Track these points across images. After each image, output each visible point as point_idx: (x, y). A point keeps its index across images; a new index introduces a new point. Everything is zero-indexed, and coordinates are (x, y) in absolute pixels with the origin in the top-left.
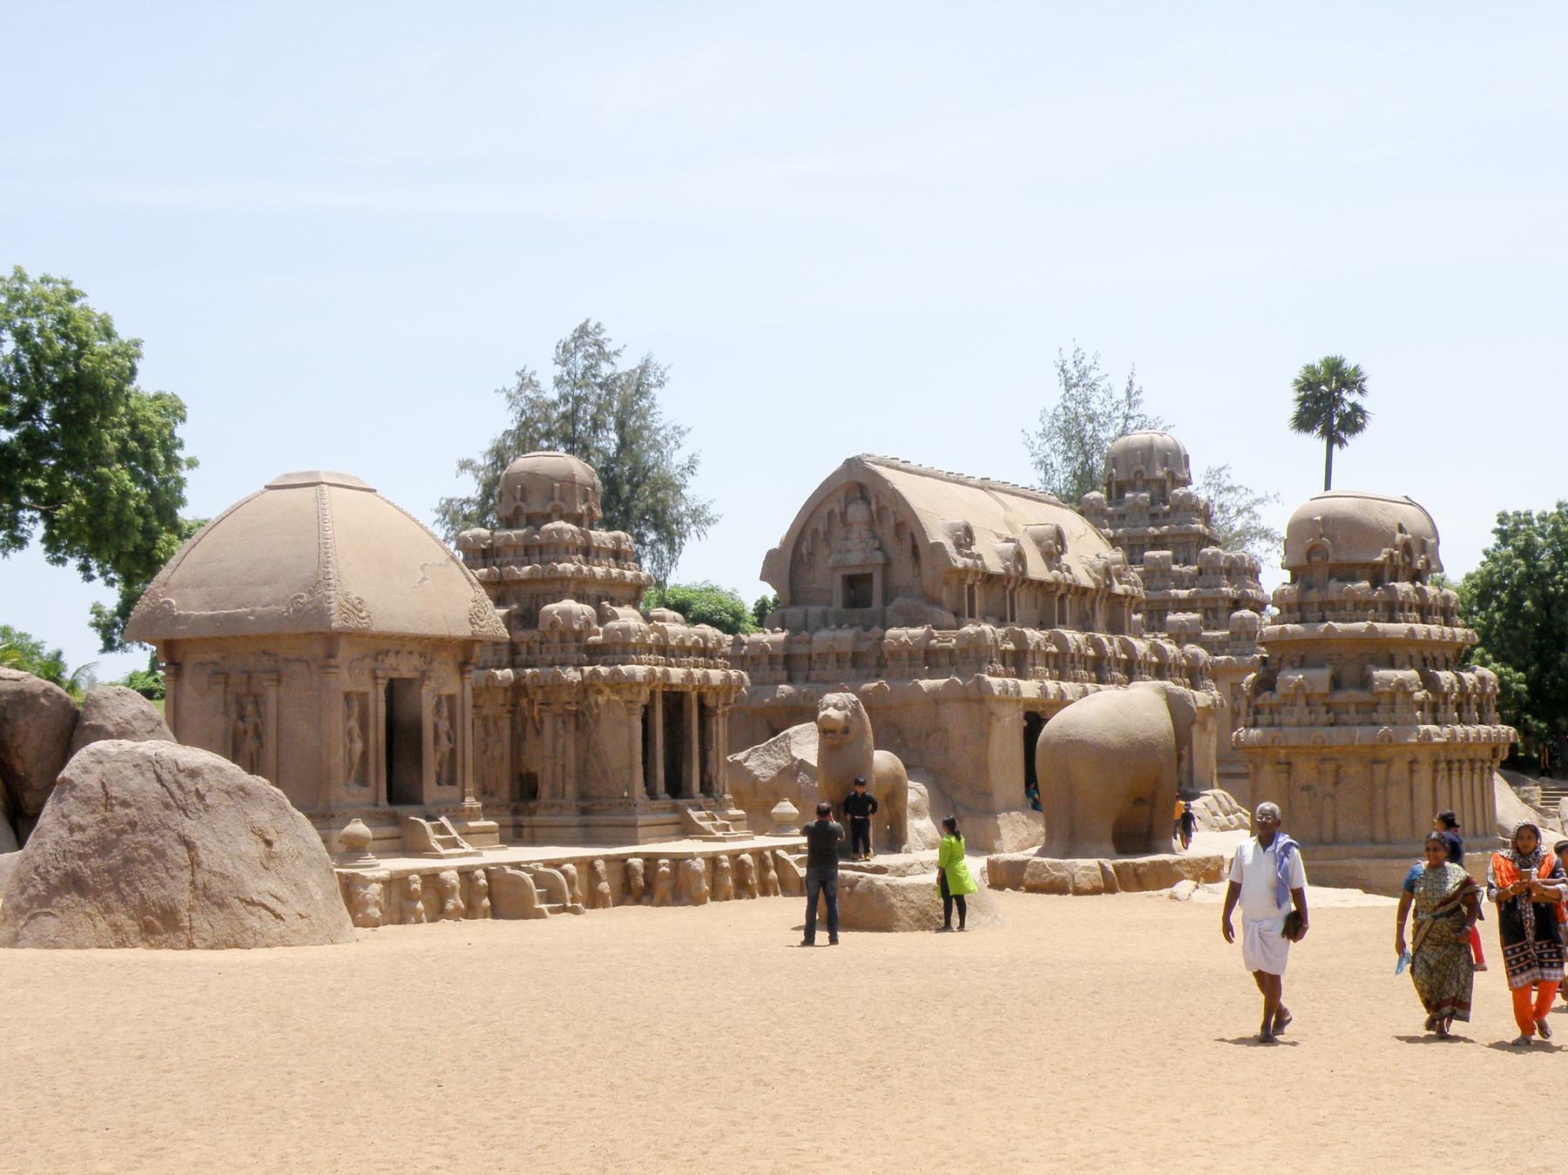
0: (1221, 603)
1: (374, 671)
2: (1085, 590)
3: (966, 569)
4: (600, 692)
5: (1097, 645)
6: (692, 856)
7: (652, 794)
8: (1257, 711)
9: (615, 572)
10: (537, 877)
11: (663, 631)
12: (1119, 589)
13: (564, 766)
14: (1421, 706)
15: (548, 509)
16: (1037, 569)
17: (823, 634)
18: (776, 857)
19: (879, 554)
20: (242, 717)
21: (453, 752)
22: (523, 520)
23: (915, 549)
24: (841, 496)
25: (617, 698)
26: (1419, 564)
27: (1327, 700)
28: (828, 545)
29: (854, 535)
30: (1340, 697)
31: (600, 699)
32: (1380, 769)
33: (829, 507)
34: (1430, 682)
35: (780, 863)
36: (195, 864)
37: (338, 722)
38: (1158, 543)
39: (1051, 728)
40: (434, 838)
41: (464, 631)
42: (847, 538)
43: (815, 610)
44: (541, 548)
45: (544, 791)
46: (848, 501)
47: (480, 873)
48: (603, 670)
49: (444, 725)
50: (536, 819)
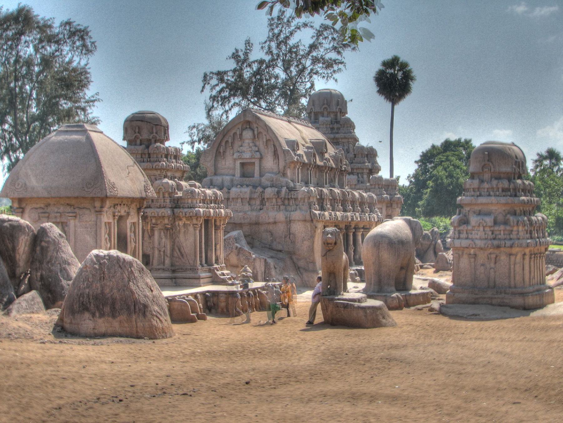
0: (365, 171)
1: (114, 213)
2: (332, 168)
4: (181, 220)
7: (201, 264)
8: (459, 233)
13: (164, 252)
18: (259, 292)
19: (258, 153)
21: (135, 246)
22: (138, 142)
24: (240, 126)
25: (189, 222)
27: (492, 229)
28: (232, 148)
29: (245, 144)
30: (496, 228)
31: (180, 223)
32: (513, 258)
33: (234, 131)
42: (241, 146)
43: (227, 178)
46: (243, 130)
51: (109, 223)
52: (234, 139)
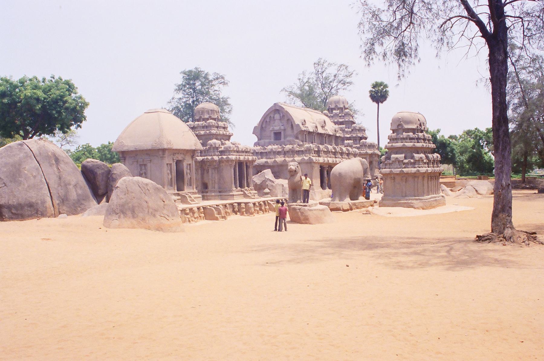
3: (305, 131)
5: (335, 148)
6: (250, 203)
7: (236, 188)
9: (225, 132)
10: (215, 208)
11: (238, 147)
12: (338, 135)
14: (425, 163)
16: (320, 131)
17: (270, 147)
18: (268, 203)
20: (141, 170)
22: (202, 120)
23: (292, 125)
26: (423, 129)
37: (166, 170)
38: (341, 123)
39: (336, 170)
40: (189, 199)
45: (210, 187)
47: (202, 208)
48: (225, 157)
49: (189, 171)
50: (208, 194)
52: (270, 119)
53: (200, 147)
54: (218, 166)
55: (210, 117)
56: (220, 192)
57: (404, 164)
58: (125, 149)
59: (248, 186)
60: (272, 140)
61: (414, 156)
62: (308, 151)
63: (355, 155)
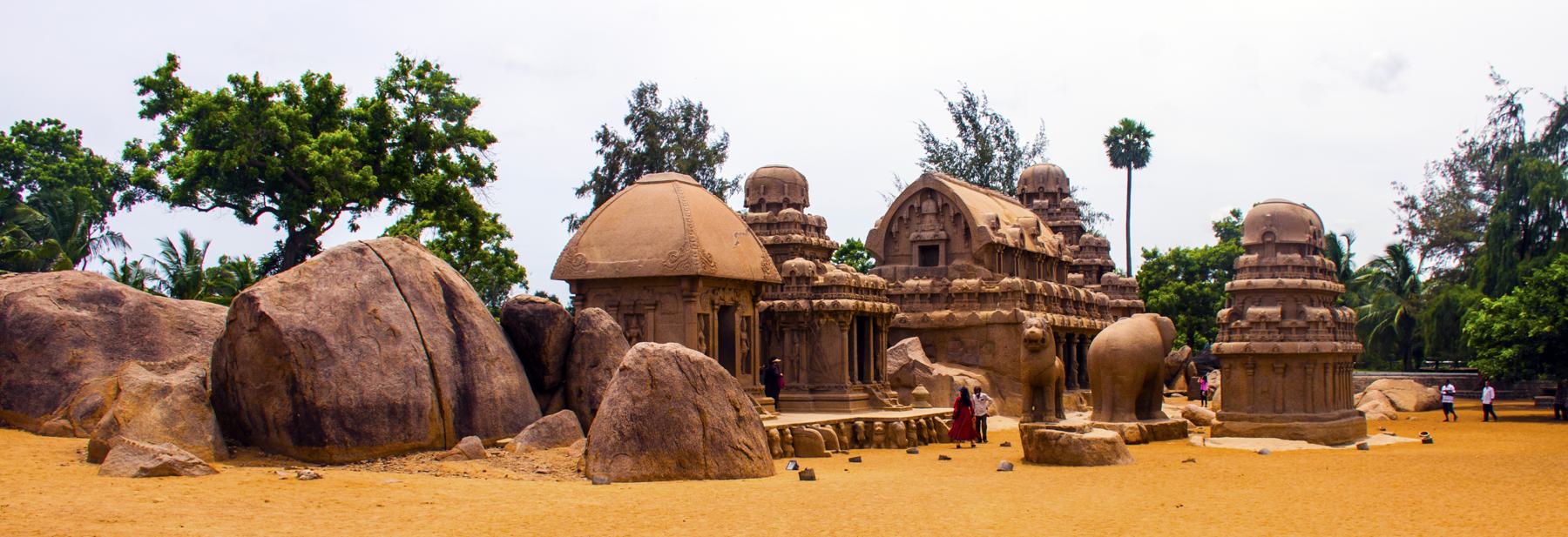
2: (1048, 258)
6: (898, 420)
7: (852, 380)
15: (781, 199)
16: (1029, 246)
17: (911, 282)
23: (967, 230)
34: (1334, 314)
35: (938, 425)
36: (704, 425)
41: (759, 276)
44: (779, 225)
48: (828, 302)
49: (745, 335)
51: (706, 316)
53: (774, 275)
54: (804, 324)
55: (786, 200)
56: (812, 391)
57: (1281, 330)
58: (590, 274)
59: (877, 378)
60: (915, 265)
61: (1303, 312)
62: (1009, 294)
63: (1139, 310)
